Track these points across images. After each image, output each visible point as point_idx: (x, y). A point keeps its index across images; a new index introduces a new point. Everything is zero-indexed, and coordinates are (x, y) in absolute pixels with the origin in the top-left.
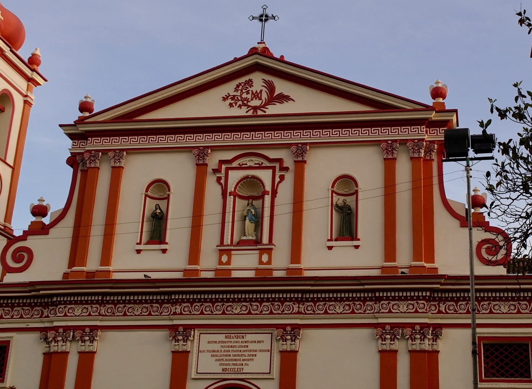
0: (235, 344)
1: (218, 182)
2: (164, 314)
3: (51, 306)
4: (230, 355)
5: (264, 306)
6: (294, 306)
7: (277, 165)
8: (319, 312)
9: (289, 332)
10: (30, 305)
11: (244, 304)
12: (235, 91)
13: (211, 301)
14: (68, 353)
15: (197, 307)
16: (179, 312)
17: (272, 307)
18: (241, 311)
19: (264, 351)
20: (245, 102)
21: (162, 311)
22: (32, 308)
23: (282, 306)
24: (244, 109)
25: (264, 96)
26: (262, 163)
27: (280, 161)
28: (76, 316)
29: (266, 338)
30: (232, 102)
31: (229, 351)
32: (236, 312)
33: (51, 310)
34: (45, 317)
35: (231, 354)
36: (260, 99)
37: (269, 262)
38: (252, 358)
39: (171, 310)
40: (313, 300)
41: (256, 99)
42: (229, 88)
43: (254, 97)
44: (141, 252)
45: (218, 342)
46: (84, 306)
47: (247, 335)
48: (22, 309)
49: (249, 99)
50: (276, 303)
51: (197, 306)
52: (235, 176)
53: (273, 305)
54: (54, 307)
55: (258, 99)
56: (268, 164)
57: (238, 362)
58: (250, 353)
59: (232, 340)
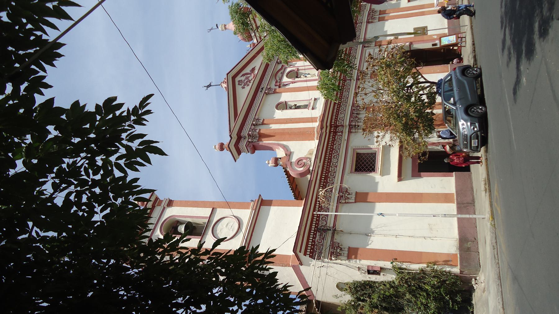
3: (336, 129)
10: (334, 140)
22: (335, 140)
24: (252, 81)
25: (249, 76)
28: (344, 116)
29: (368, 51)
30: (246, 85)
33: (339, 130)
34: (342, 134)
36: (250, 77)
42: (238, 88)
44: (314, 107)
46: (339, 114)
48: (335, 144)
52: (285, 79)
54: (337, 129)
56: (283, 70)
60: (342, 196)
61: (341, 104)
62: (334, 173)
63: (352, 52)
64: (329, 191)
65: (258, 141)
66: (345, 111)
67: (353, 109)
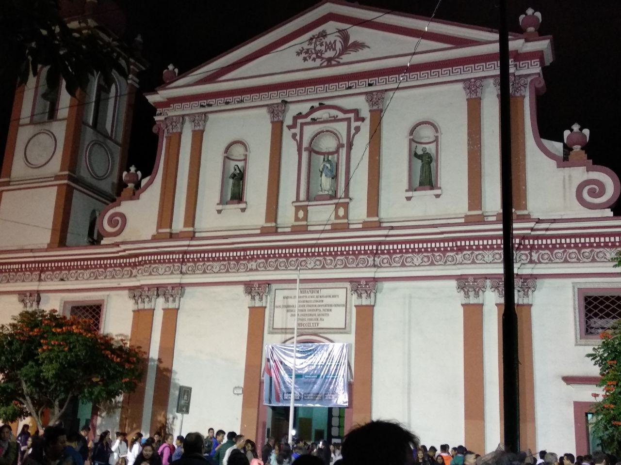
0: (310, 299)
1: (293, 138)
2: (240, 270)
3: (139, 265)
4: (305, 310)
5: (338, 259)
6: (369, 259)
7: (352, 115)
8: (395, 264)
9: (363, 286)
11: (318, 258)
12: (309, 44)
13: (285, 256)
14: (154, 309)
15: (271, 263)
16: (255, 268)
17: (346, 261)
18: (315, 266)
19: (338, 305)
20: (319, 54)
21: (239, 269)
23: (357, 259)
24: (318, 62)
25: (339, 46)
26: (337, 116)
27: (356, 112)
29: (342, 293)
31: (304, 306)
32: (310, 267)
35: (307, 308)
36: (334, 49)
37: (346, 216)
38: (327, 312)
39: (247, 266)
40: (389, 252)
41: (330, 50)
43: (328, 48)
44: (222, 212)
45: (293, 297)
46: (167, 265)
47: (322, 290)
48: (114, 270)
49: (323, 51)
50: (350, 257)
51: (272, 262)
53: (347, 258)
55: (332, 50)
57: (314, 317)
58: (325, 308)
59: (307, 295)
60: (27, 296)
61: (189, 264)
62: (68, 279)
63: (339, 258)
64: (40, 276)
65: (166, 137)
66: (172, 273)
67: (167, 287)
